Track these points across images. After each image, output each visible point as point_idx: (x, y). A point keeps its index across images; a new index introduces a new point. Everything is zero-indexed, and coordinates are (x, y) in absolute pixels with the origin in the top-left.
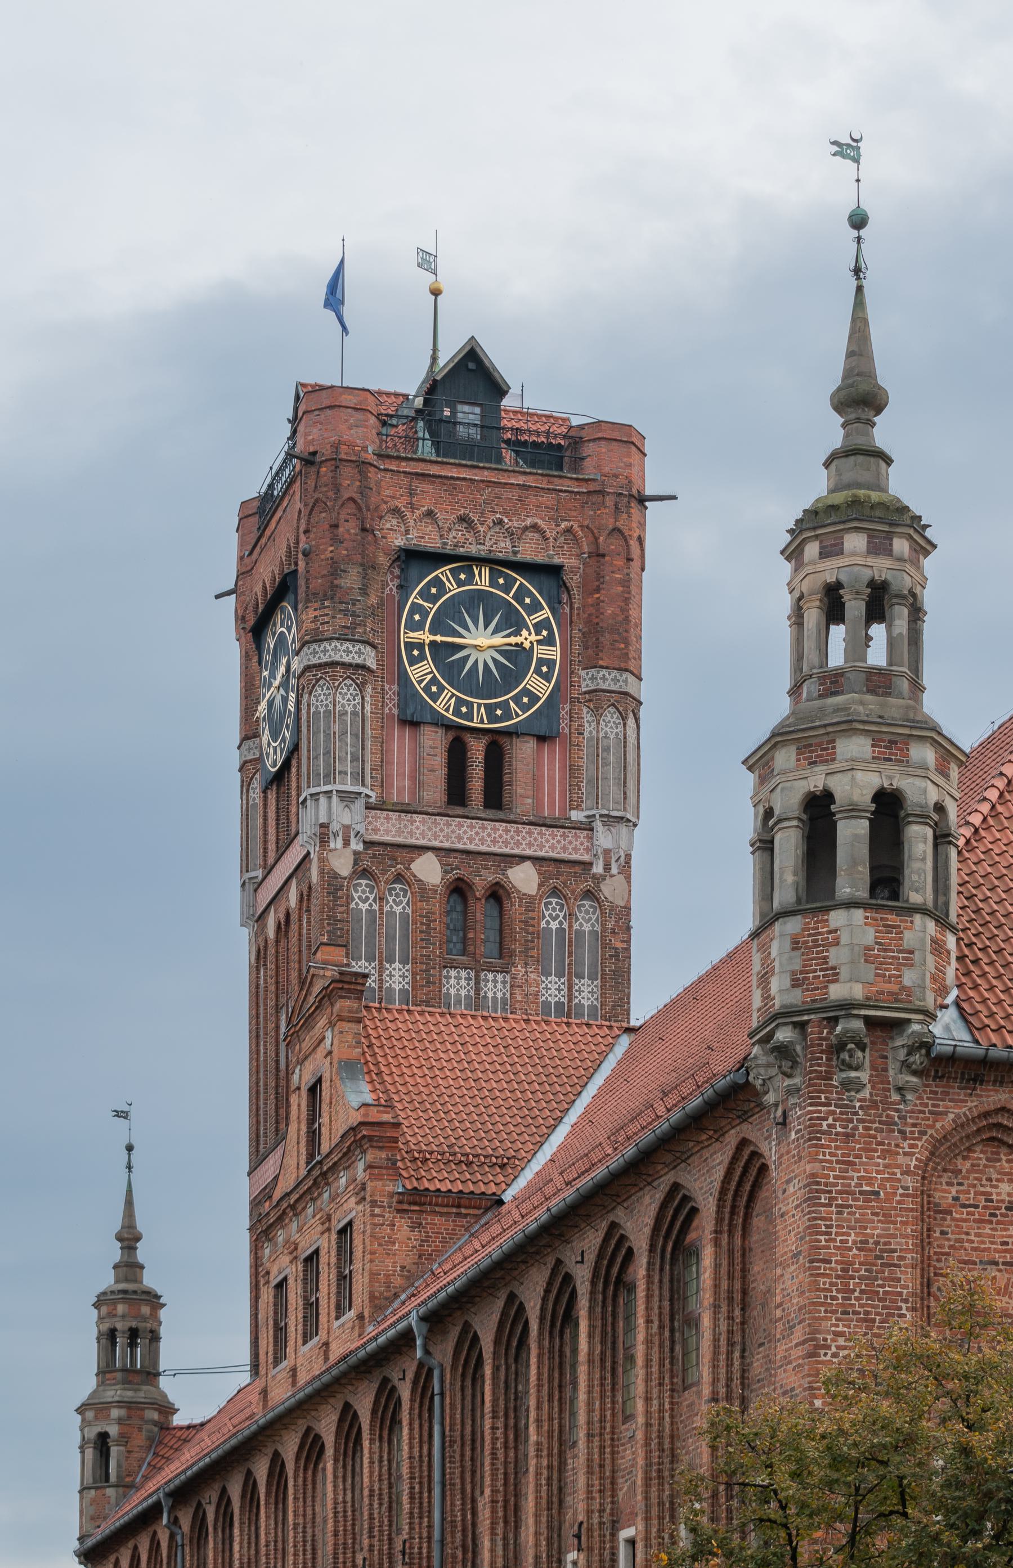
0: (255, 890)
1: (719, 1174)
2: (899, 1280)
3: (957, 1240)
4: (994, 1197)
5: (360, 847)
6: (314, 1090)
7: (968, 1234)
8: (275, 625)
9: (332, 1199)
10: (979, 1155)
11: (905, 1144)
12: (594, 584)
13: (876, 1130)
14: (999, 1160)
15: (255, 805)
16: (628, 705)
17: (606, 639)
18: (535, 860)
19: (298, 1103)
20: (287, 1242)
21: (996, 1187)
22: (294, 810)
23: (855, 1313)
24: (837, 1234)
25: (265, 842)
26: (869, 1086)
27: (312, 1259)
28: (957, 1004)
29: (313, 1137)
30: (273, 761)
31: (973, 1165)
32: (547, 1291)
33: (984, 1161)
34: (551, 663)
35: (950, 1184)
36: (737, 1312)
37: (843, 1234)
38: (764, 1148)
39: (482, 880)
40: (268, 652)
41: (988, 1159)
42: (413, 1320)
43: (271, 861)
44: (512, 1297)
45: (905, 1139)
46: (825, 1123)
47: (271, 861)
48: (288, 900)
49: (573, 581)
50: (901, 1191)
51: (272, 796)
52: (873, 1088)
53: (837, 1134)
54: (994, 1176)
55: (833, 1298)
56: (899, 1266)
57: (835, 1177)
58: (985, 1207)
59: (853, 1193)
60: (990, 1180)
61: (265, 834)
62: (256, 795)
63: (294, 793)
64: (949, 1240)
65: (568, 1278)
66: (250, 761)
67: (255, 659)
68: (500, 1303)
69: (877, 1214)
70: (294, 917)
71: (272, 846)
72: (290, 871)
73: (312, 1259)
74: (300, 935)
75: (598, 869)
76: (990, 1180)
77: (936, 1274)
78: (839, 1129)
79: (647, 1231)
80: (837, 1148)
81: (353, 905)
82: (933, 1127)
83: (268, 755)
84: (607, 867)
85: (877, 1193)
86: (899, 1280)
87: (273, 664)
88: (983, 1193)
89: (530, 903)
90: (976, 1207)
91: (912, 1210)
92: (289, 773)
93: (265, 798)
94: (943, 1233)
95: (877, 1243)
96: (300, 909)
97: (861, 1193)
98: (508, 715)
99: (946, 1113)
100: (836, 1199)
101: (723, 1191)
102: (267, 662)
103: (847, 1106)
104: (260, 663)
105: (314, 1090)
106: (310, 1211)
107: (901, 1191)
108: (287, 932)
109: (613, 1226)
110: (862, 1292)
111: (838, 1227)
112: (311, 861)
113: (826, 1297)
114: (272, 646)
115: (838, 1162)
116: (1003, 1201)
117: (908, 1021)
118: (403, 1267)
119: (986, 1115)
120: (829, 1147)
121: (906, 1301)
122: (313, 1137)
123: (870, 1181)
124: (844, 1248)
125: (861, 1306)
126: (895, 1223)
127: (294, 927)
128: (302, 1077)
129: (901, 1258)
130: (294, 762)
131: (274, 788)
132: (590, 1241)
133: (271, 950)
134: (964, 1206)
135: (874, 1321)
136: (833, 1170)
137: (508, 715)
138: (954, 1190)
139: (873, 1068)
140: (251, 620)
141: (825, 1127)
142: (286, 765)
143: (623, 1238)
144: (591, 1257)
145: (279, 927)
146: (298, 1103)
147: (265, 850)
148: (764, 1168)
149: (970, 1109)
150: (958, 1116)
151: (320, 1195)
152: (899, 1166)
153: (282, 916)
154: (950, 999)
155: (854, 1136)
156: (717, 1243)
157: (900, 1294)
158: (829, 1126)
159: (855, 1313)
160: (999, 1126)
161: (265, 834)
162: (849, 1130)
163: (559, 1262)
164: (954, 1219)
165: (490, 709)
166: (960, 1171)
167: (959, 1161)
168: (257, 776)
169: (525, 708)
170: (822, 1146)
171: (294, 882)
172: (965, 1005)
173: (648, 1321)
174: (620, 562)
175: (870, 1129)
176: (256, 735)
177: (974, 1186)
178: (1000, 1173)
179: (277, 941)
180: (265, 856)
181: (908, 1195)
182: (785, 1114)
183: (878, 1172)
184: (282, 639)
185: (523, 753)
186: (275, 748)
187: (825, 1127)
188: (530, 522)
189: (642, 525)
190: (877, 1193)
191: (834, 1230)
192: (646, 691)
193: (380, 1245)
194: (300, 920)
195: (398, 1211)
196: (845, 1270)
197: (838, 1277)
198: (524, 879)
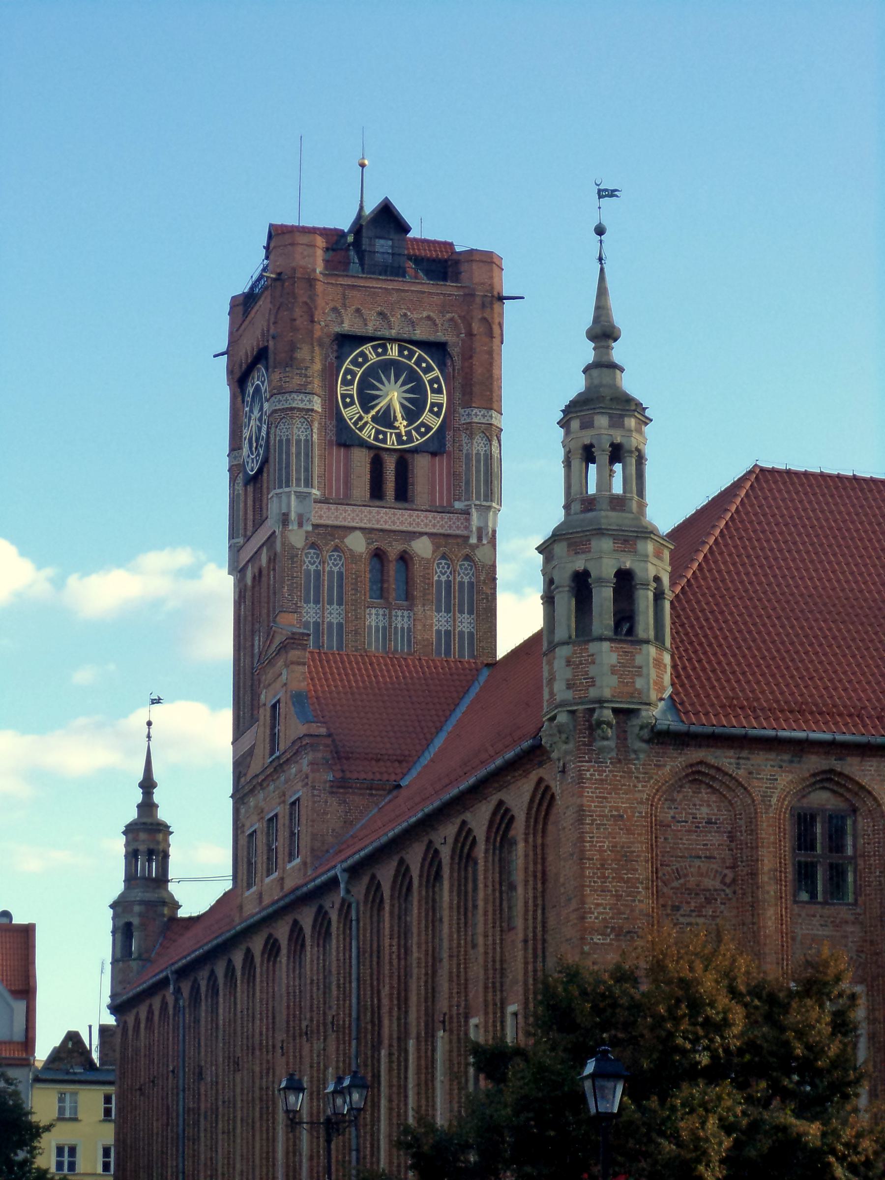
0: (238, 551)
1: (527, 797)
2: (637, 870)
3: (675, 844)
4: (698, 816)
5: (310, 528)
7: (681, 839)
8: (253, 378)
9: (287, 781)
10: (688, 790)
11: (640, 785)
13: (621, 776)
14: (700, 792)
15: (238, 495)
20: (256, 807)
21: (699, 809)
22: (265, 501)
23: (609, 891)
24: (597, 842)
25: (246, 519)
26: (616, 750)
28: (670, 696)
30: (252, 468)
31: (684, 796)
32: (424, 859)
33: (691, 794)
35: (670, 808)
36: (539, 885)
37: (601, 842)
38: (552, 784)
40: (249, 396)
41: (694, 792)
42: (338, 871)
43: (249, 533)
44: (402, 861)
45: (639, 782)
46: (588, 773)
47: (249, 533)
48: (260, 560)
50: (637, 814)
51: (250, 489)
52: (619, 751)
53: (596, 780)
54: (698, 802)
55: (594, 882)
56: (637, 861)
57: (595, 807)
58: (693, 822)
59: (606, 816)
60: (695, 805)
61: (246, 513)
62: (240, 488)
63: (265, 491)
64: (669, 843)
65: (436, 852)
66: (236, 465)
67: (240, 399)
68: (394, 864)
69: (622, 829)
70: (265, 572)
71: (250, 523)
72: (263, 541)
74: (269, 585)
76: (695, 805)
77: (661, 865)
78: (597, 777)
79: (485, 828)
80: (596, 788)
81: (305, 567)
82: (657, 774)
83: (248, 463)
85: (622, 816)
86: (637, 870)
87: (251, 405)
88: (691, 814)
90: (686, 822)
91: (645, 826)
92: (262, 476)
93: (246, 490)
94: (666, 839)
95: (623, 847)
96: (269, 567)
97: (611, 816)
99: (665, 766)
100: (596, 820)
101: (530, 808)
102: (248, 402)
103: (602, 762)
104: (243, 402)
106: (272, 787)
107: (637, 814)
108: (260, 581)
109: (464, 823)
110: (613, 878)
111: (598, 837)
112: (276, 537)
113: (590, 882)
114: (251, 392)
115: (597, 797)
116: (703, 818)
117: (639, 709)
118: (333, 830)
119: (691, 765)
120: (591, 788)
121: (642, 883)
123: (617, 809)
124: (601, 851)
125: (614, 887)
126: (634, 834)
127: (264, 579)
129: (638, 856)
130: (265, 470)
131: (252, 484)
132: (449, 830)
133: (249, 594)
134: (679, 822)
135: (621, 896)
136: (593, 802)
138: (672, 812)
139: (618, 737)
140: (238, 375)
141: (588, 776)
142: (260, 471)
143: (470, 831)
144: (450, 841)
145: (254, 578)
147: (246, 524)
148: (553, 796)
149: (680, 763)
150: (672, 766)
151: (278, 778)
152: (636, 799)
153: (256, 571)
154: (666, 695)
155: (606, 780)
156: (526, 841)
157: (638, 879)
158: (591, 775)
159: (609, 891)
160: (699, 772)
161: (246, 513)
162: (603, 777)
163: (431, 842)
164: (673, 830)
166: (676, 800)
167: (675, 794)
168: (241, 475)
170: (587, 787)
171: (265, 550)
172: (675, 697)
173: (486, 886)
175: (617, 776)
176: (240, 448)
177: (685, 809)
178: (701, 801)
179: (253, 587)
180: (245, 529)
181: (642, 817)
182: (564, 765)
183: (622, 803)
184: (257, 389)
186: (253, 459)
187: (588, 776)
190: (622, 816)
191: (595, 839)
193: (318, 815)
194: (269, 575)
195: (332, 793)
196: (603, 865)
197: (598, 869)
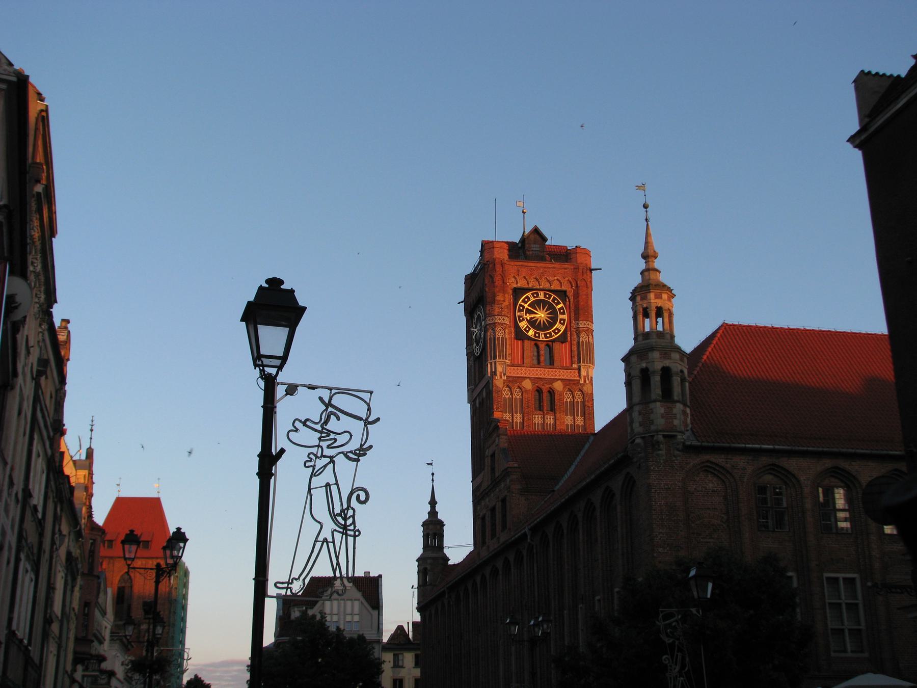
6: (493, 455)
12: (576, 295)
16: (590, 332)
17: (581, 312)
18: (562, 380)
19: (488, 461)
27: (493, 510)
29: (493, 469)
34: (564, 320)
39: (545, 388)
42: (526, 530)
49: (570, 294)
62: (472, 363)
73: (493, 510)
75: (582, 382)
84: (585, 381)
89: (561, 394)
98: (551, 336)
105: (493, 455)
122: (493, 469)
128: (488, 452)
137: (551, 336)
142: (481, 353)
146: (488, 461)
165: (545, 335)
169: (556, 334)
174: (585, 289)
185: (557, 346)
188: (558, 277)
189: (591, 277)
192: (595, 327)
198: (558, 386)
